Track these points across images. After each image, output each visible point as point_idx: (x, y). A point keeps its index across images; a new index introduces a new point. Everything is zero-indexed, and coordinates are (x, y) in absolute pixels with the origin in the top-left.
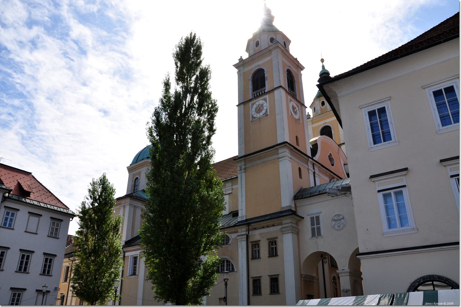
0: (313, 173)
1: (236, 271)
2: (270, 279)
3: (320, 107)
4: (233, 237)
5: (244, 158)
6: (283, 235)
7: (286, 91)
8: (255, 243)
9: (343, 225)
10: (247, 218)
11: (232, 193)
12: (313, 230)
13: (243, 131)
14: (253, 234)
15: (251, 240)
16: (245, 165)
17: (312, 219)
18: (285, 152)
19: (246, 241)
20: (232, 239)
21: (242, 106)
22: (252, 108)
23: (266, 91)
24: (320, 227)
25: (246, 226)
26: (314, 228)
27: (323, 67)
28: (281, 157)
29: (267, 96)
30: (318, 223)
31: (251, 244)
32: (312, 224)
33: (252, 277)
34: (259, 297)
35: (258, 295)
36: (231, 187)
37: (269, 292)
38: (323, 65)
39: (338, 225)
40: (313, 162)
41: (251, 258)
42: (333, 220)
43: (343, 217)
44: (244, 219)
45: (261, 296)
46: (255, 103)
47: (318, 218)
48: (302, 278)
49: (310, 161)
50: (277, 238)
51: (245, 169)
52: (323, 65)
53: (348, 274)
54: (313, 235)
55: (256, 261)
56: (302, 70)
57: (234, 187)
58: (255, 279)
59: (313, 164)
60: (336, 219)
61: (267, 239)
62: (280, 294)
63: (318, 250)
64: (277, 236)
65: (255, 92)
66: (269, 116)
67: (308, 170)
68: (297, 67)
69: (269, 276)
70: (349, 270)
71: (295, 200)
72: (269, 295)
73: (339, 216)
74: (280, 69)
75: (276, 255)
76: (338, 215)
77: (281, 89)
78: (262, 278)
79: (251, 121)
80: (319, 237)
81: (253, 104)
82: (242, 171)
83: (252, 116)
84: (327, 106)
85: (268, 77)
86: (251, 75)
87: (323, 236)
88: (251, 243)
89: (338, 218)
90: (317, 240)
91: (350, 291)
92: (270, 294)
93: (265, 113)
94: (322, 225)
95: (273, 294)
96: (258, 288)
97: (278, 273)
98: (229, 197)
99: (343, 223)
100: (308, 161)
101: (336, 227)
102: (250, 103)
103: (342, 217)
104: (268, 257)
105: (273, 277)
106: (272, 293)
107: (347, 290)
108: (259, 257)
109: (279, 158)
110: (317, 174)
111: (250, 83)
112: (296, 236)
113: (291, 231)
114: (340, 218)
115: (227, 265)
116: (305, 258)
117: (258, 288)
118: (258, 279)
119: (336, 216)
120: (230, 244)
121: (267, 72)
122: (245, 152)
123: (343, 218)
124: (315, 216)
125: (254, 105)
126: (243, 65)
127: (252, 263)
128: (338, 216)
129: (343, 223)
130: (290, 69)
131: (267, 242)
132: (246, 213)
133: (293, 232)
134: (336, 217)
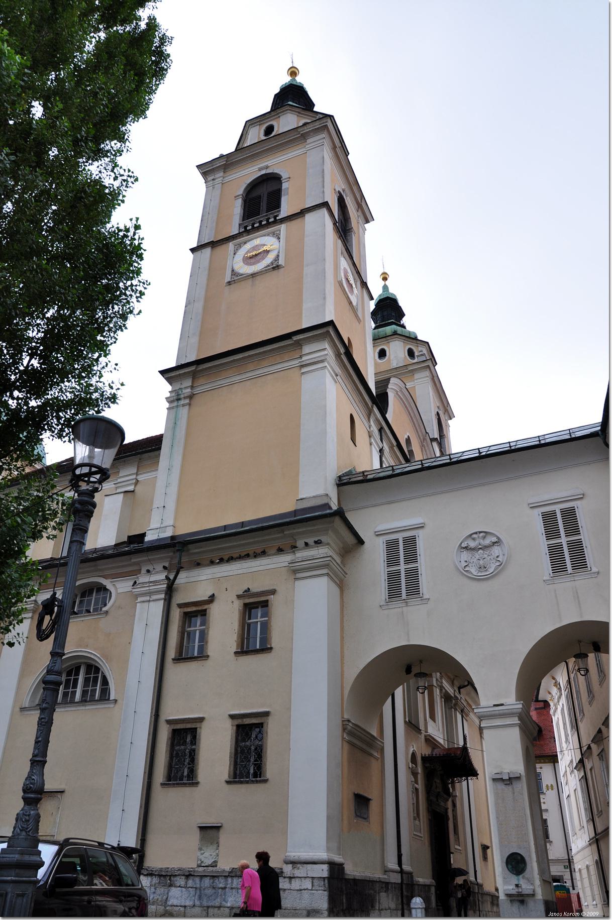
0: (378, 450)
1: (116, 701)
2: (235, 728)
3: (375, 360)
4: (120, 591)
5: (193, 368)
6: (297, 583)
7: (335, 224)
8: (194, 609)
9: (498, 564)
10: (177, 534)
11: (133, 491)
12: (393, 579)
13: (199, 306)
14: (192, 580)
15: (179, 598)
16: (192, 387)
17: (392, 546)
18: (325, 350)
19: (162, 602)
20: (118, 594)
21: (207, 251)
22: (235, 254)
23: (283, 214)
24: (416, 570)
25: (171, 554)
26: (399, 572)
27: (385, 288)
28: (308, 362)
29: (283, 227)
30: (412, 556)
31: (180, 612)
32: (392, 560)
33: (169, 722)
34: (187, 790)
35: (185, 784)
36: (134, 477)
37: (226, 776)
38: (385, 284)
39: (481, 562)
40: (380, 424)
41: (173, 657)
42: (464, 548)
43: (498, 538)
44: (169, 533)
45: (193, 789)
46: (245, 243)
47: (411, 543)
48: (345, 736)
49: (375, 415)
50: (273, 592)
51: (191, 397)
52: (385, 284)
53: (516, 721)
54: (393, 592)
55: (193, 665)
56: (367, 221)
57: (140, 478)
58: (179, 727)
59: (381, 430)
60: (472, 544)
61: (239, 597)
62: (266, 781)
63: (409, 641)
64: (271, 588)
65: (246, 222)
66: (281, 270)
67: (370, 437)
68: (357, 207)
69: (232, 717)
70: (521, 706)
71: (340, 488)
72: (224, 782)
73: (484, 538)
74: (325, 171)
75: (266, 649)
76: (480, 532)
77: (324, 211)
78: (205, 725)
79: (229, 283)
80: (413, 601)
81: (239, 246)
82: (182, 402)
83: (233, 271)
84: (391, 358)
85: (290, 190)
86: (245, 186)
87: (425, 597)
88: (178, 610)
89: (482, 541)
90: (405, 609)
91: (524, 779)
92: (228, 782)
93: (272, 263)
94: (423, 564)
95: (241, 782)
96: (187, 761)
97: (267, 710)
98: (123, 498)
99: (498, 557)
100: (370, 415)
101: (473, 570)
102: (231, 245)
103: (494, 539)
104: (236, 653)
105: (248, 721)
106: (235, 776)
107: (511, 776)
108: (203, 656)
109: (302, 366)
110: (386, 458)
111: (239, 202)
112: (336, 590)
113: (325, 571)
114: (487, 542)
115: (87, 681)
116: (362, 667)
117: (187, 761)
118: (189, 726)
119: (474, 536)
120: (107, 612)
121: (289, 178)
122: (197, 355)
123: (498, 542)
124: (400, 537)
125: (240, 247)
126: (225, 169)
127: (176, 673)
128: (482, 534)
129: (498, 557)
130: (345, 197)
131: (238, 605)
132: (175, 519)
133: (330, 573)
134: (474, 539)
